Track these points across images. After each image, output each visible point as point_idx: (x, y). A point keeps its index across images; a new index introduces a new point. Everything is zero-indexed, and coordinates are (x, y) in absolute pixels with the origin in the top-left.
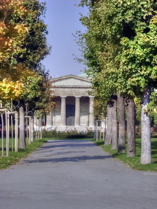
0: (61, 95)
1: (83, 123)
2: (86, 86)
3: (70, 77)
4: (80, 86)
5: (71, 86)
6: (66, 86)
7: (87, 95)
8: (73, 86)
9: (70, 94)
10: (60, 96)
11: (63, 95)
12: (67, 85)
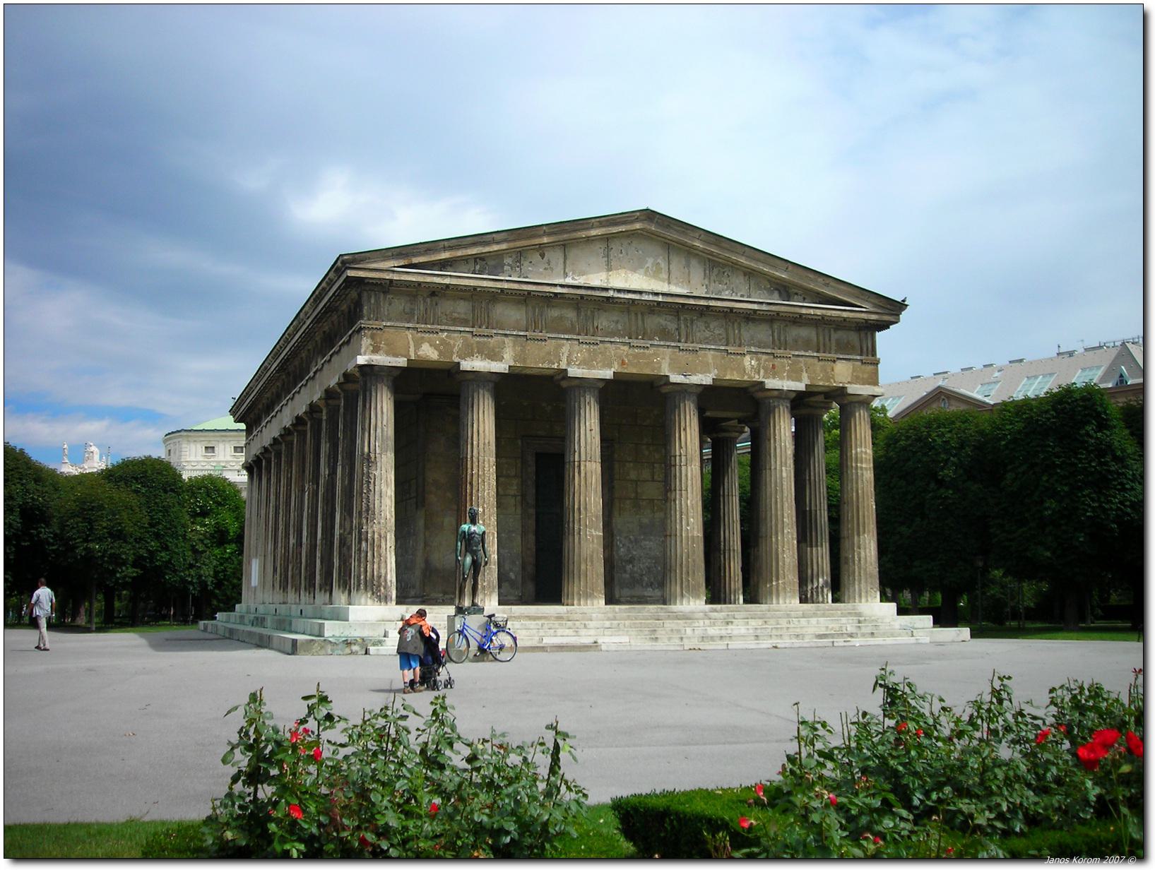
0: (569, 364)
1: (651, 585)
2: (755, 307)
4: (712, 303)
5: (645, 297)
6: (611, 293)
7: (749, 367)
8: (660, 299)
9: (636, 356)
10: (563, 366)
11: (586, 363)
12: (619, 291)
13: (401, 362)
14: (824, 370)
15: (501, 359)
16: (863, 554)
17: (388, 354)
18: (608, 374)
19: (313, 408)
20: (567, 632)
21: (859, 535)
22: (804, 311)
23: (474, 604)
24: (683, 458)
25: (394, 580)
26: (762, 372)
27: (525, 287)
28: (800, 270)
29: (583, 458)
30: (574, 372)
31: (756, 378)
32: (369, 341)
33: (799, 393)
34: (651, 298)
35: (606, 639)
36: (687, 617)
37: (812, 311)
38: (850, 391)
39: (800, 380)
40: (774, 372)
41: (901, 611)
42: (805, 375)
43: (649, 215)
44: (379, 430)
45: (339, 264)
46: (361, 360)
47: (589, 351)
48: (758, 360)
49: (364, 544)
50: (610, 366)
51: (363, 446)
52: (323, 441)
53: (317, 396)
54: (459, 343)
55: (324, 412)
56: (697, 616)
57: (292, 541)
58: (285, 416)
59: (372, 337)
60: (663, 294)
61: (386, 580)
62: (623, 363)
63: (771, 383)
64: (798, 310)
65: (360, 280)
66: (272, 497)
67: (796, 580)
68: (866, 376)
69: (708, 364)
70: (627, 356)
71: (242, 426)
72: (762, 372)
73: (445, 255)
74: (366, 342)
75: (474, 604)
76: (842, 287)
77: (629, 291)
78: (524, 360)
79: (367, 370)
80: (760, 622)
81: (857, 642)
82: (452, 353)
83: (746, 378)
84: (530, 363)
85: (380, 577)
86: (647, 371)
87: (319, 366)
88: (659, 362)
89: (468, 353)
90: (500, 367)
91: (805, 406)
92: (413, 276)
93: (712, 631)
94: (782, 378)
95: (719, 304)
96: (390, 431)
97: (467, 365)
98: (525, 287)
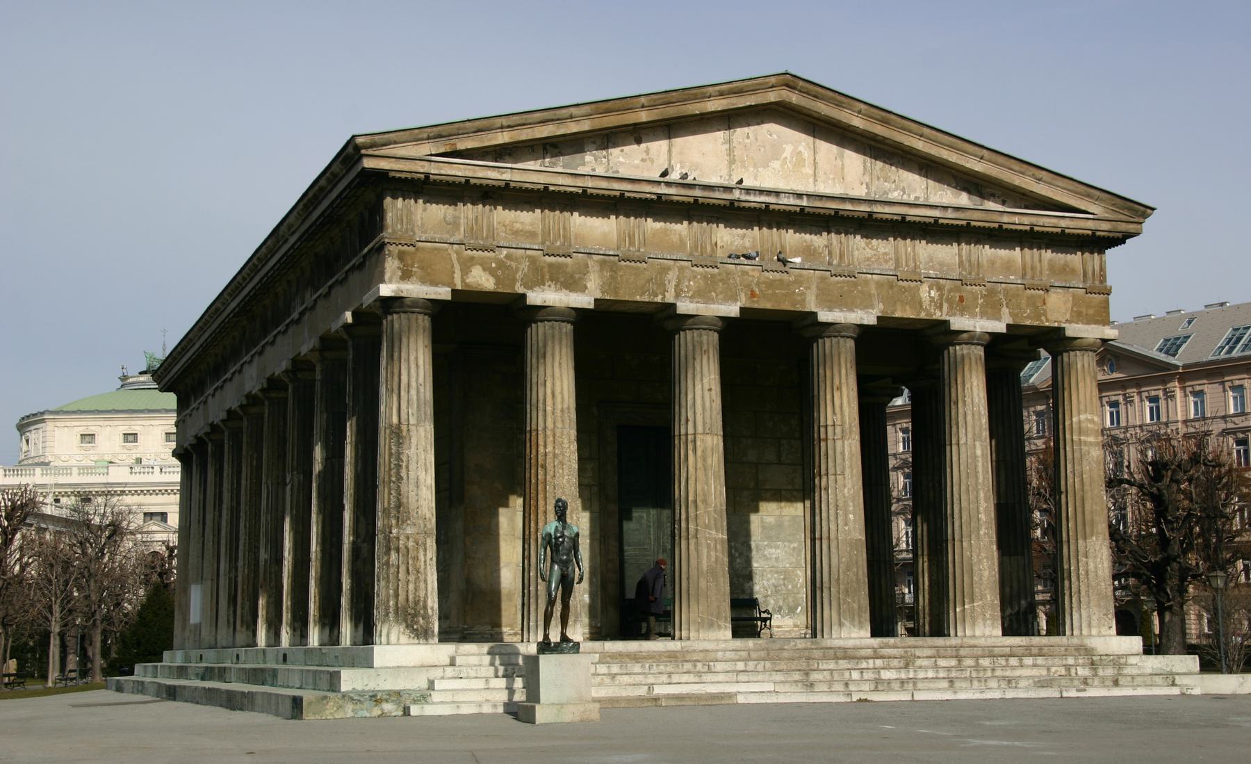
0: (677, 295)
2: (936, 213)
3: (772, 97)
4: (878, 209)
5: (785, 201)
6: (736, 195)
7: (926, 303)
8: (804, 202)
9: (771, 284)
10: (670, 299)
11: (701, 295)
12: (748, 191)
13: (443, 293)
14: (1031, 302)
15: (583, 289)
16: (1091, 566)
17: (423, 281)
18: (732, 310)
19: (299, 365)
20: (685, 678)
21: (1085, 538)
22: (1005, 219)
23: (565, 638)
24: (838, 430)
25: (436, 606)
26: (945, 306)
27: (616, 185)
28: (1001, 159)
29: (700, 429)
30: (684, 307)
31: (938, 315)
32: (396, 263)
33: (995, 336)
34: (792, 201)
35: (742, 688)
36: (846, 654)
37: (1016, 219)
38: (1069, 333)
39: (999, 319)
40: (962, 305)
41: (1147, 651)
42: (1005, 310)
43: (790, 81)
44: (413, 392)
45: (350, 150)
46: (386, 290)
47: (705, 277)
48: (940, 289)
49: (393, 555)
50: (734, 298)
51: (388, 413)
52: (317, 410)
53: (307, 345)
54: (525, 266)
55: (318, 369)
56: (863, 653)
57: (263, 556)
58: (250, 378)
59: (401, 256)
60: (809, 196)
61: (425, 607)
62: (753, 294)
63: (957, 323)
64: (996, 217)
65: (382, 175)
66: (226, 496)
67: (997, 602)
68: (1091, 312)
69: (870, 295)
70: (758, 284)
71: (171, 399)
72: (945, 306)
73: (503, 138)
74: (391, 265)
75: (565, 638)
76: (1061, 182)
77: (761, 192)
78: (616, 291)
79: (392, 304)
80: (953, 662)
81: (1092, 692)
82: (514, 280)
83: (923, 316)
84: (624, 295)
85: (416, 603)
86: (786, 306)
87: (309, 301)
88: (803, 294)
89: (537, 280)
90: (584, 300)
91: (1006, 353)
92: (458, 170)
93: (886, 675)
94: (973, 316)
95: (887, 209)
96: (428, 393)
97: (535, 297)
98: (616, 185)
